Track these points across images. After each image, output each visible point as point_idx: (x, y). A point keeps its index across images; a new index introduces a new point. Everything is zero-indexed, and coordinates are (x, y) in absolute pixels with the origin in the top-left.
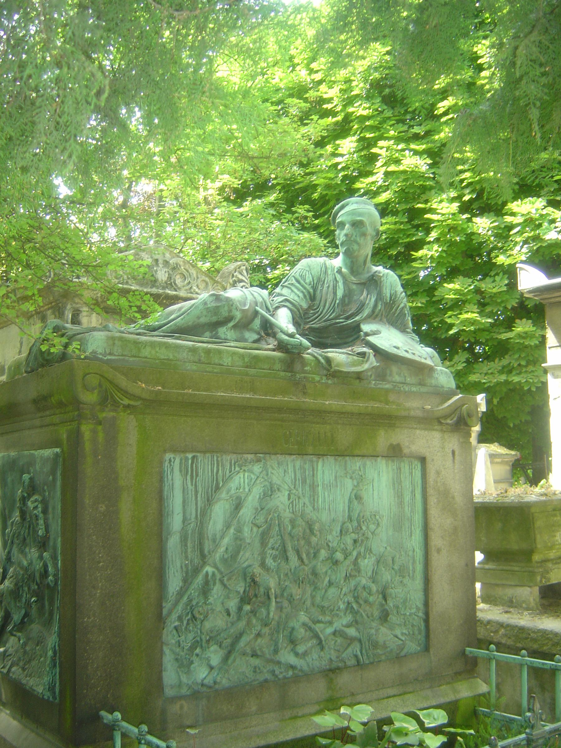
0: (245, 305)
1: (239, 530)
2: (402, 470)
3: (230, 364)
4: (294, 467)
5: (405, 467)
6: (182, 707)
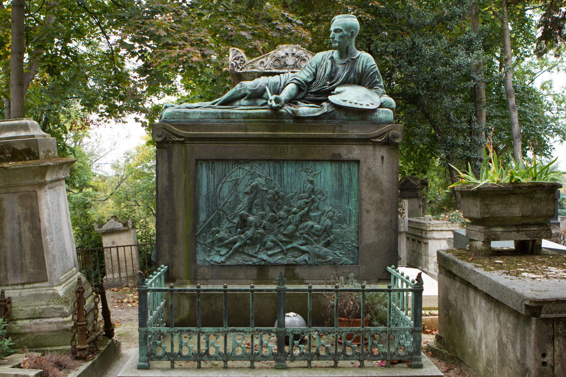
0: (256, 86)
1: (237, 196)
2: (343, 167)
6: (204, 270)
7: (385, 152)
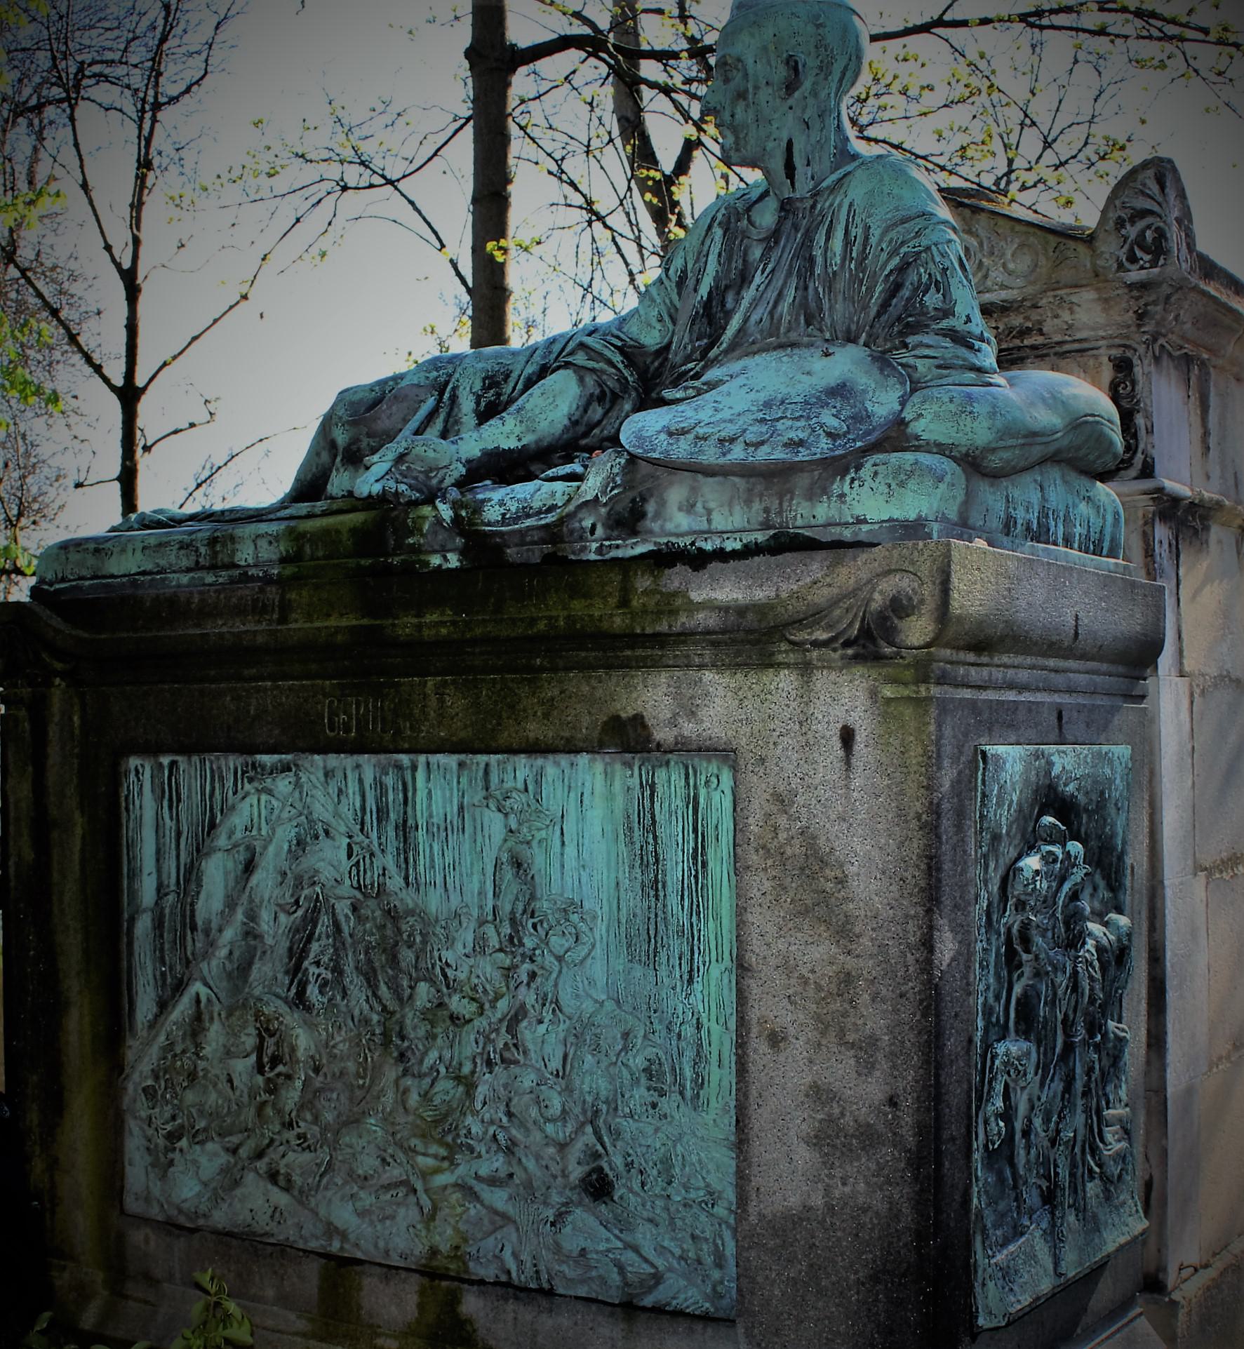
1: (252, 916)
2: (659, 789)
3: (251, 561)
4: (361, 781)
5: (670, 782)
6: (147, 1241)
7: (862, 698)
